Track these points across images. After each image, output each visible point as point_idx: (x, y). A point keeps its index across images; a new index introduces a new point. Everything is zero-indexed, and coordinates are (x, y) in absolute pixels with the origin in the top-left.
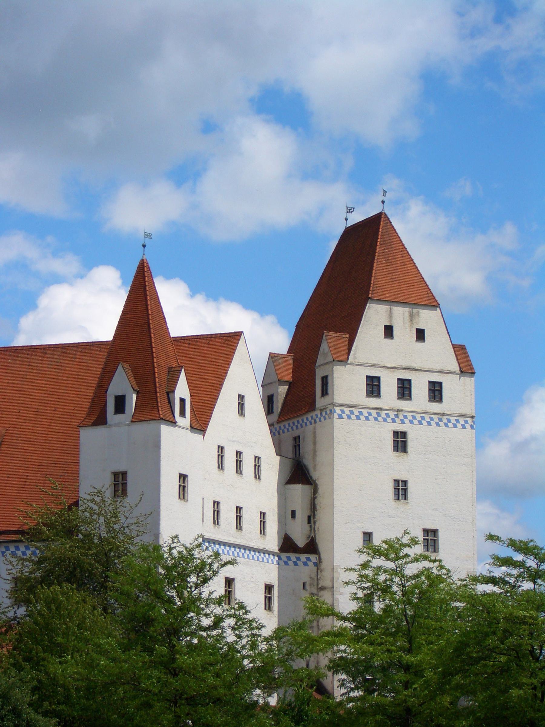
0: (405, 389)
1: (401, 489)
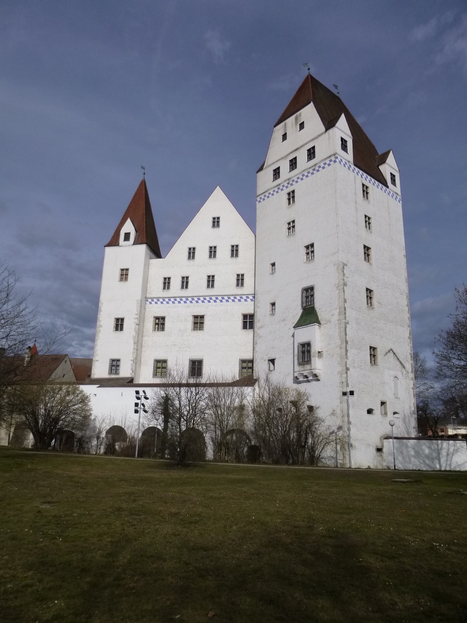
0: (293, 164)
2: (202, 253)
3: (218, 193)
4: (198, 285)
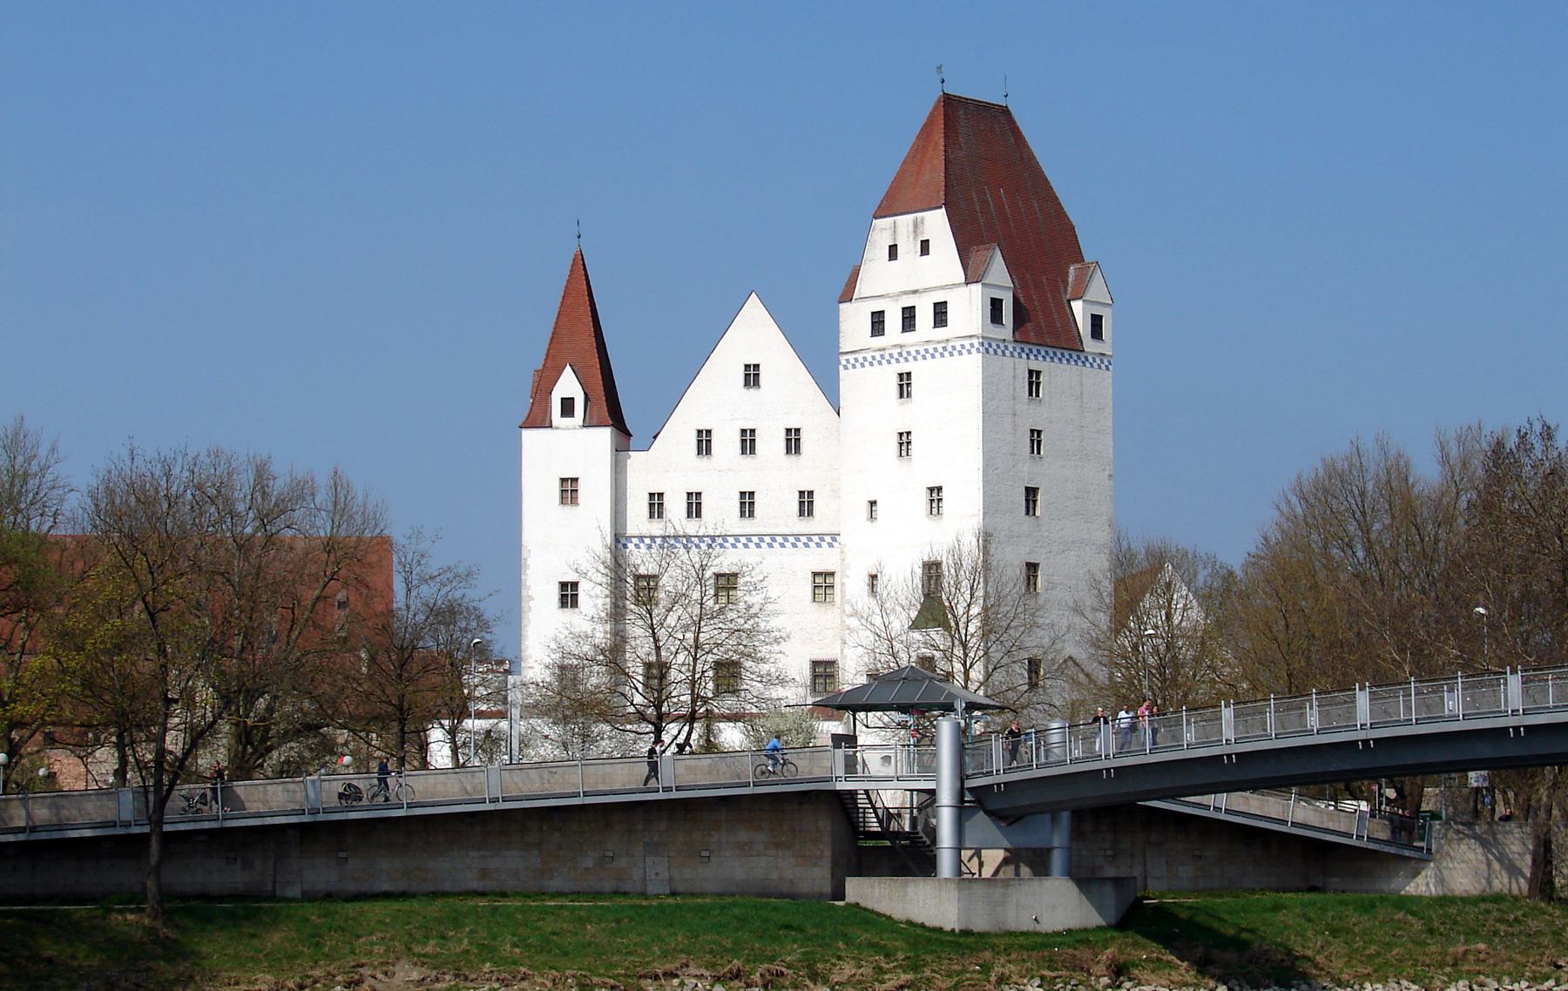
1: (905, 441)
2: (726, 443)
3: (754, 308)
4: (721, 512)
